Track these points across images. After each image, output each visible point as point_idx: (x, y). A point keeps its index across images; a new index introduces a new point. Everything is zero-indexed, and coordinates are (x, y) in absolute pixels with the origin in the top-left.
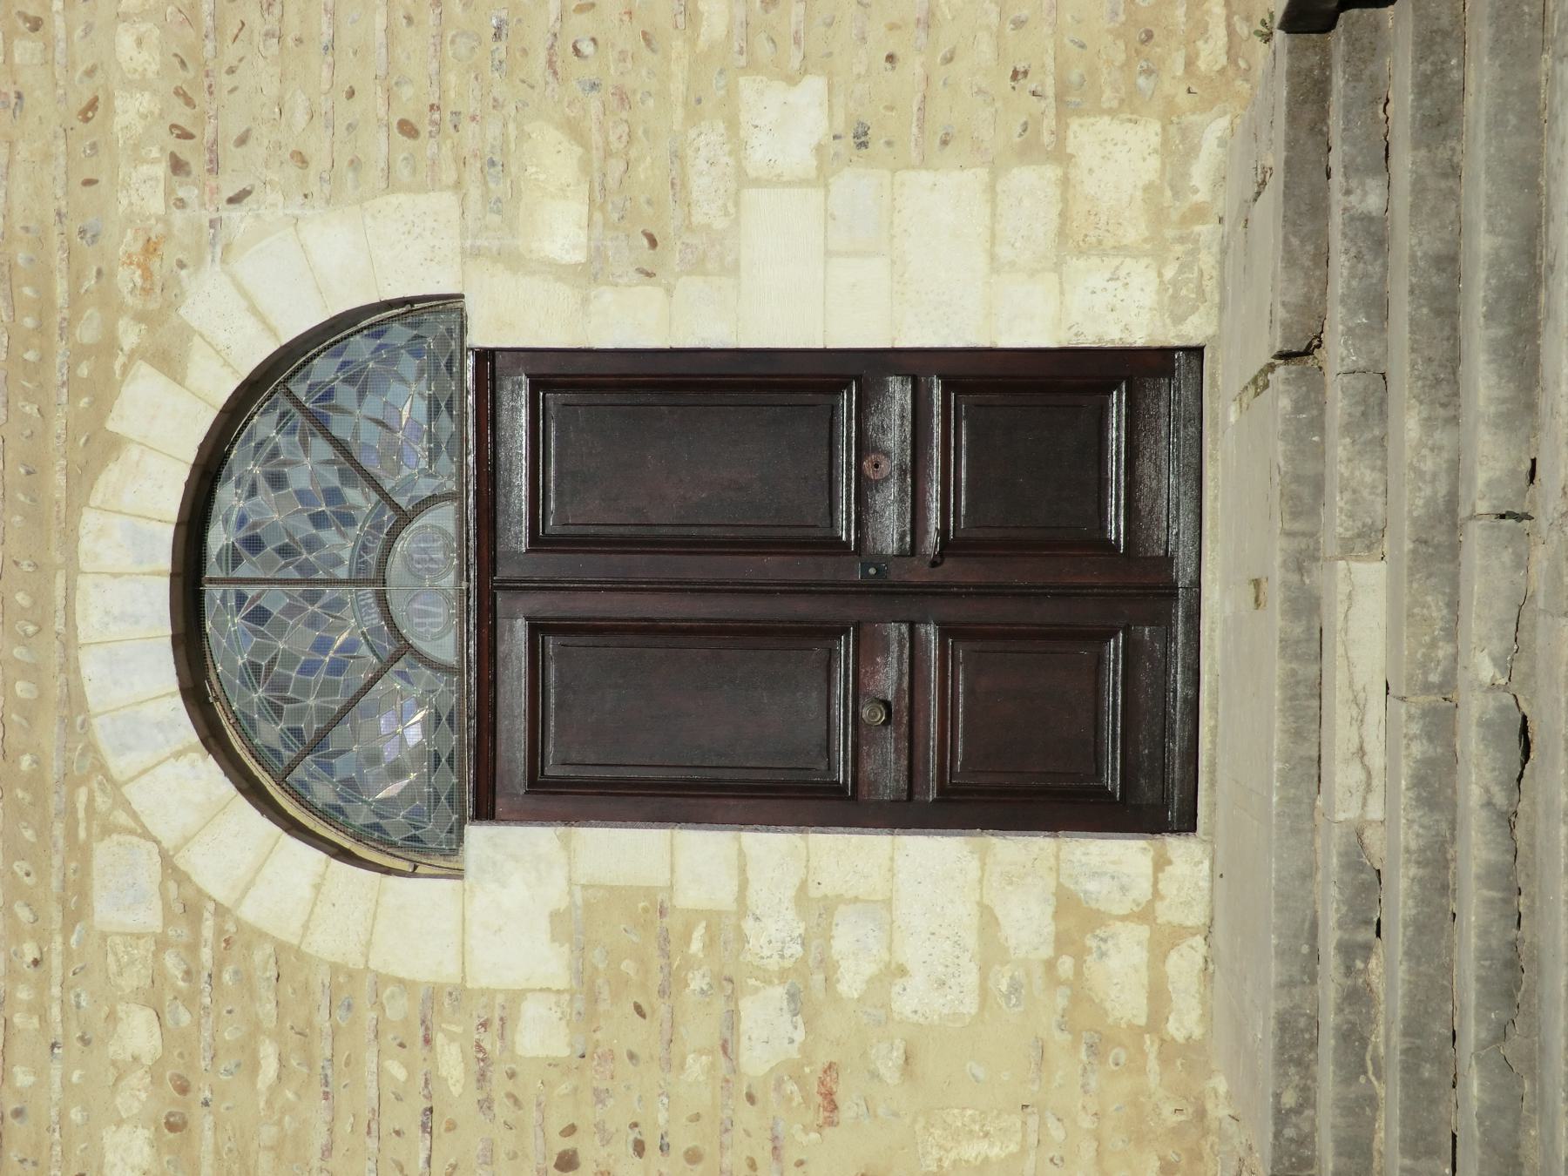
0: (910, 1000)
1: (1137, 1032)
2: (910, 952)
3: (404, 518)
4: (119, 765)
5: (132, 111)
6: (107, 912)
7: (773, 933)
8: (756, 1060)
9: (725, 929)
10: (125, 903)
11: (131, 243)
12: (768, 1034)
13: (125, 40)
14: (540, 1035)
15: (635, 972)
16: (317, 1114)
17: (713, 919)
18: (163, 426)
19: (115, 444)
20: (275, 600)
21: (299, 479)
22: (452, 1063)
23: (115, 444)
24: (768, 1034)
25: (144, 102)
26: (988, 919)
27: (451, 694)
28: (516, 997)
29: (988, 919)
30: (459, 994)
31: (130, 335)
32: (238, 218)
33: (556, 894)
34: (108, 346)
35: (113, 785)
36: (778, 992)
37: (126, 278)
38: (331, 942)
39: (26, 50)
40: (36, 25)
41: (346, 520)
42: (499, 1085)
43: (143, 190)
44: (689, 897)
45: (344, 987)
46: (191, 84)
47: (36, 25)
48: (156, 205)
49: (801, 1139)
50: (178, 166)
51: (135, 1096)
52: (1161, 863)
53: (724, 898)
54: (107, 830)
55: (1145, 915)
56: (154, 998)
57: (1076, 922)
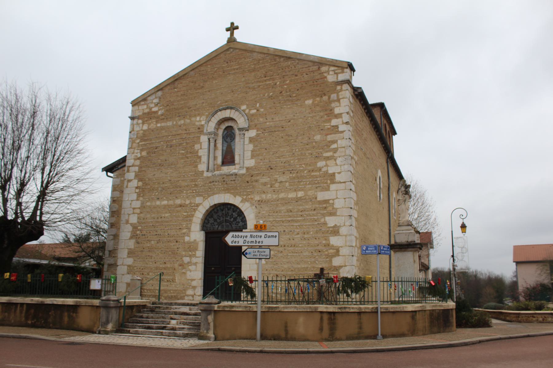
0: (188, 273)
1: (185, 293)
2: (192, 272)
3: (230, 224)
4: (209, 199)
5: (264, 196)
6: (197, 198)
7: (194, 260)
8: (184, 258)
9: (194, 256)
10: (198, 200)
11: (252, 197)
12: (186, 260)
13: (270, 195)
14: (187, 239)
15: (191, 248)
16: (181, 219)
17: (195, 255)
18: (236, 201)
19: (235, 197)
20: (224, 212)
21: (234, 214)
22: (184, 231)
23: (235, 197)
24: (186, 260)
25: (264, 198)
26: (194, 280)
27: (216, 229)
28: (189, 236)
29: (194, 280)
30: (190, 231)
31: (245, 197)
32: (254, 207)
33: (198, 240)
34: (244, 195)
35: (207, 198)
36: (189, 260)
37: (249, 197)
38: (194, 219)
39: (269, 186)
40: (271, 187)
41: (230, 218)
42: (183, 235)
43: (257, 198)
44: (197, 252)
45: (191, 220)
46: (266, 202)
47: (271, 187)
48: (256, 199)
49: (178, 263)
50: (259, 201)
51: (183, 202)
52: (199, 296)
53: (197, 256)
54: (204, 198)
55: (195, 294)
56: (191, 203)
57: (194, 288)
